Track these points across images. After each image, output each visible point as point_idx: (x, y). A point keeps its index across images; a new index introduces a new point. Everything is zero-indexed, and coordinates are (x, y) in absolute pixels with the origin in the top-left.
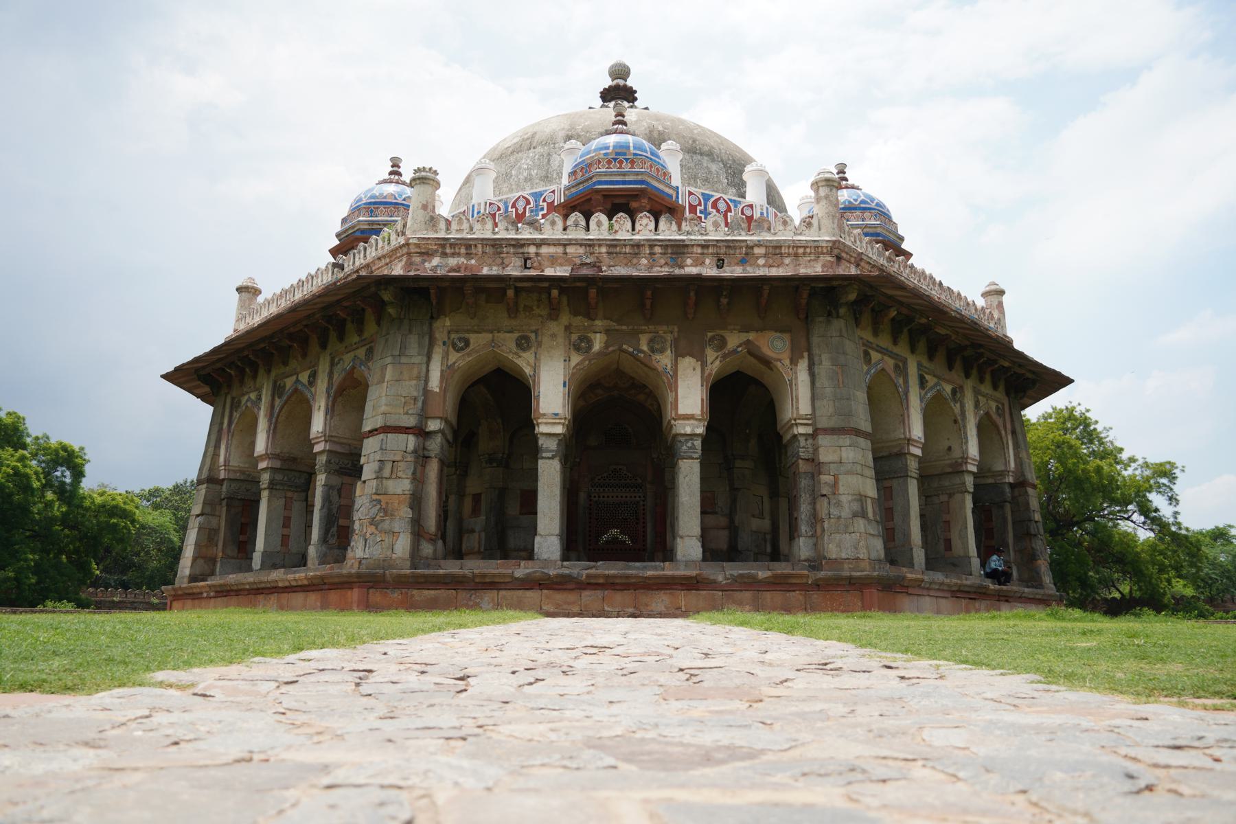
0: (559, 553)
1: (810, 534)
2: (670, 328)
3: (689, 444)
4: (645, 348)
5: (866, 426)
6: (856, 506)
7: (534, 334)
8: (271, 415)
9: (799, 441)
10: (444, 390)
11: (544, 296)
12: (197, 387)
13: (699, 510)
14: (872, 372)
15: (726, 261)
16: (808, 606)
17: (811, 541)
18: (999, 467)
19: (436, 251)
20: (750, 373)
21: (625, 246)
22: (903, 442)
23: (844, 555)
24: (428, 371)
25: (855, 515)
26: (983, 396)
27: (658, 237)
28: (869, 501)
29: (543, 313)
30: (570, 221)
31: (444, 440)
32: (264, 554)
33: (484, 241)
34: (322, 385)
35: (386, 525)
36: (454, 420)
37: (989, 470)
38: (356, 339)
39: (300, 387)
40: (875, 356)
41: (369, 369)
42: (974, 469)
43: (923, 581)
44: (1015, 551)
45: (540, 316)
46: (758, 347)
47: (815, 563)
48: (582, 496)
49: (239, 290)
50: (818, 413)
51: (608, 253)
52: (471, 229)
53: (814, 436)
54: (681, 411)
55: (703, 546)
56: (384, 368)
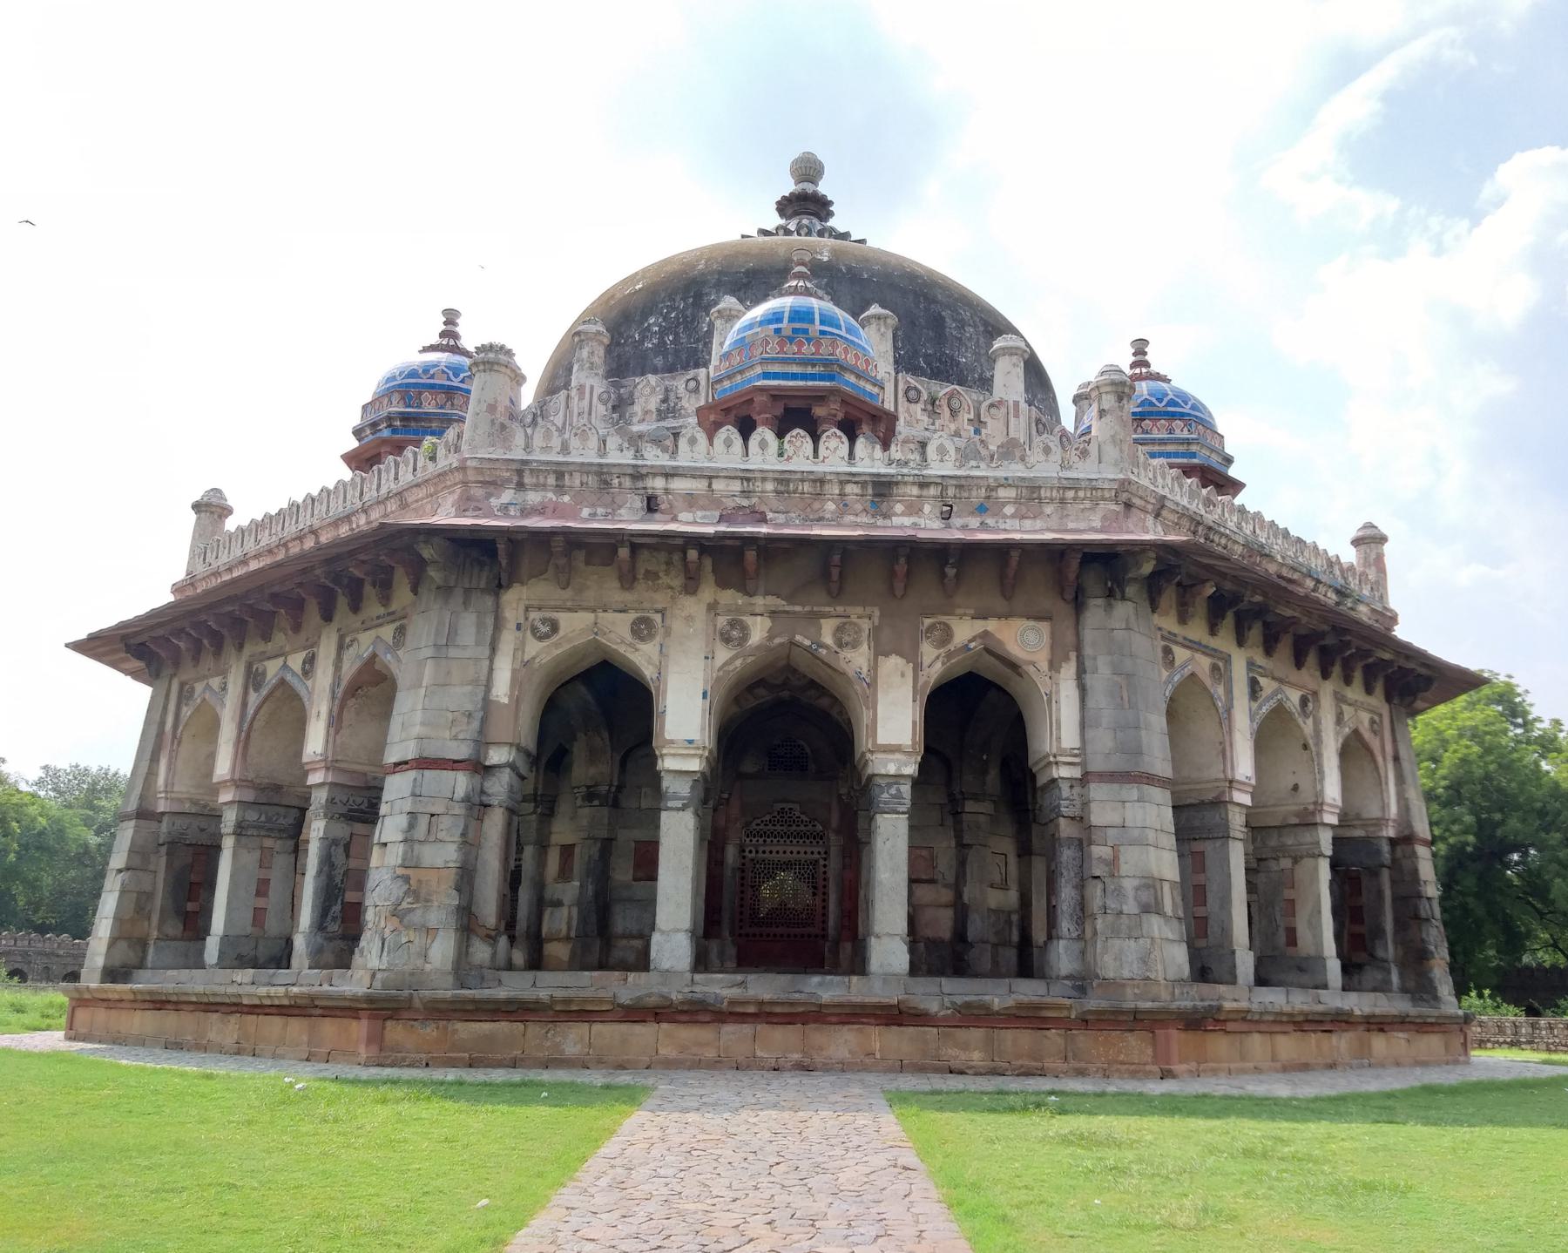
0: (688, 960)
1: (1074, 935)
2: (869, 610)
3: (893, 791)
4: (828, 639)
5: (1163, 768)
7: (660, 615)
9: (1060, 789)
10: (517, 701)
11: (676, 557)
12: (123, 660)
13: (905, 876)
14: (1176, 679)
15: (955, 509)
16: (1070, 1055)
17: (1078, 946)
18: (1373, 811)
19: (509, 481)
20: (989, 676)
21: (803, 481)
22: (1222, 784)
23: (1126, 974)
24: (491, 670)
25: (1145, 909)
26: (1350, 705)
27: (854, 470)
28: (1166, 887)
29: (673, 584)
31: (514, 776)
33: (584, 468)
34: (323, 677)
36: (531, 745)
37: (1358, 817)
38: (382, 611)
39: (289, 677)
40: (1181, 654)
41: (399, 661)
42: (1334, 820)
43: (1249, 1011)
44: (1395, 943)
45: (672, 588)
46: (1000, 642)
47: (1082, 983)
49: (197, 507)
50: (1089, 749)
51: (777, 492)
52: (565, 449)
53: (1085, 780)
54: (881, 741)
55: (912, 951)
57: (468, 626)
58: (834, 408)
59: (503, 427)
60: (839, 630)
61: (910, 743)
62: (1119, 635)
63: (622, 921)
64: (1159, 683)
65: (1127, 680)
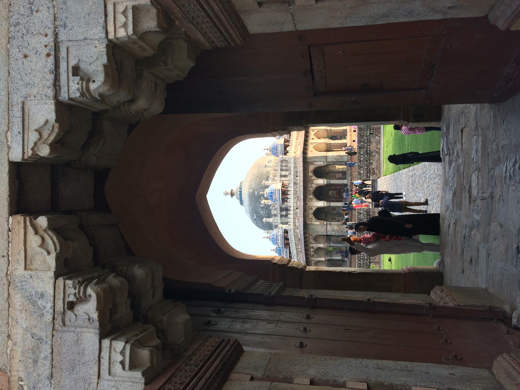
4: (312, 189)
8: (318, 257)
10: (319, 222)
14: (314, 150)
30: (289, 202)
33: (294, 216)
35: (342, 229)
38: (308, 238)
48: (333, 199)
53: (327, 162)
57: (311, 227)
58: (283, 188)
59: (289, 225)
60: (311, 188)
61: (323, 180)
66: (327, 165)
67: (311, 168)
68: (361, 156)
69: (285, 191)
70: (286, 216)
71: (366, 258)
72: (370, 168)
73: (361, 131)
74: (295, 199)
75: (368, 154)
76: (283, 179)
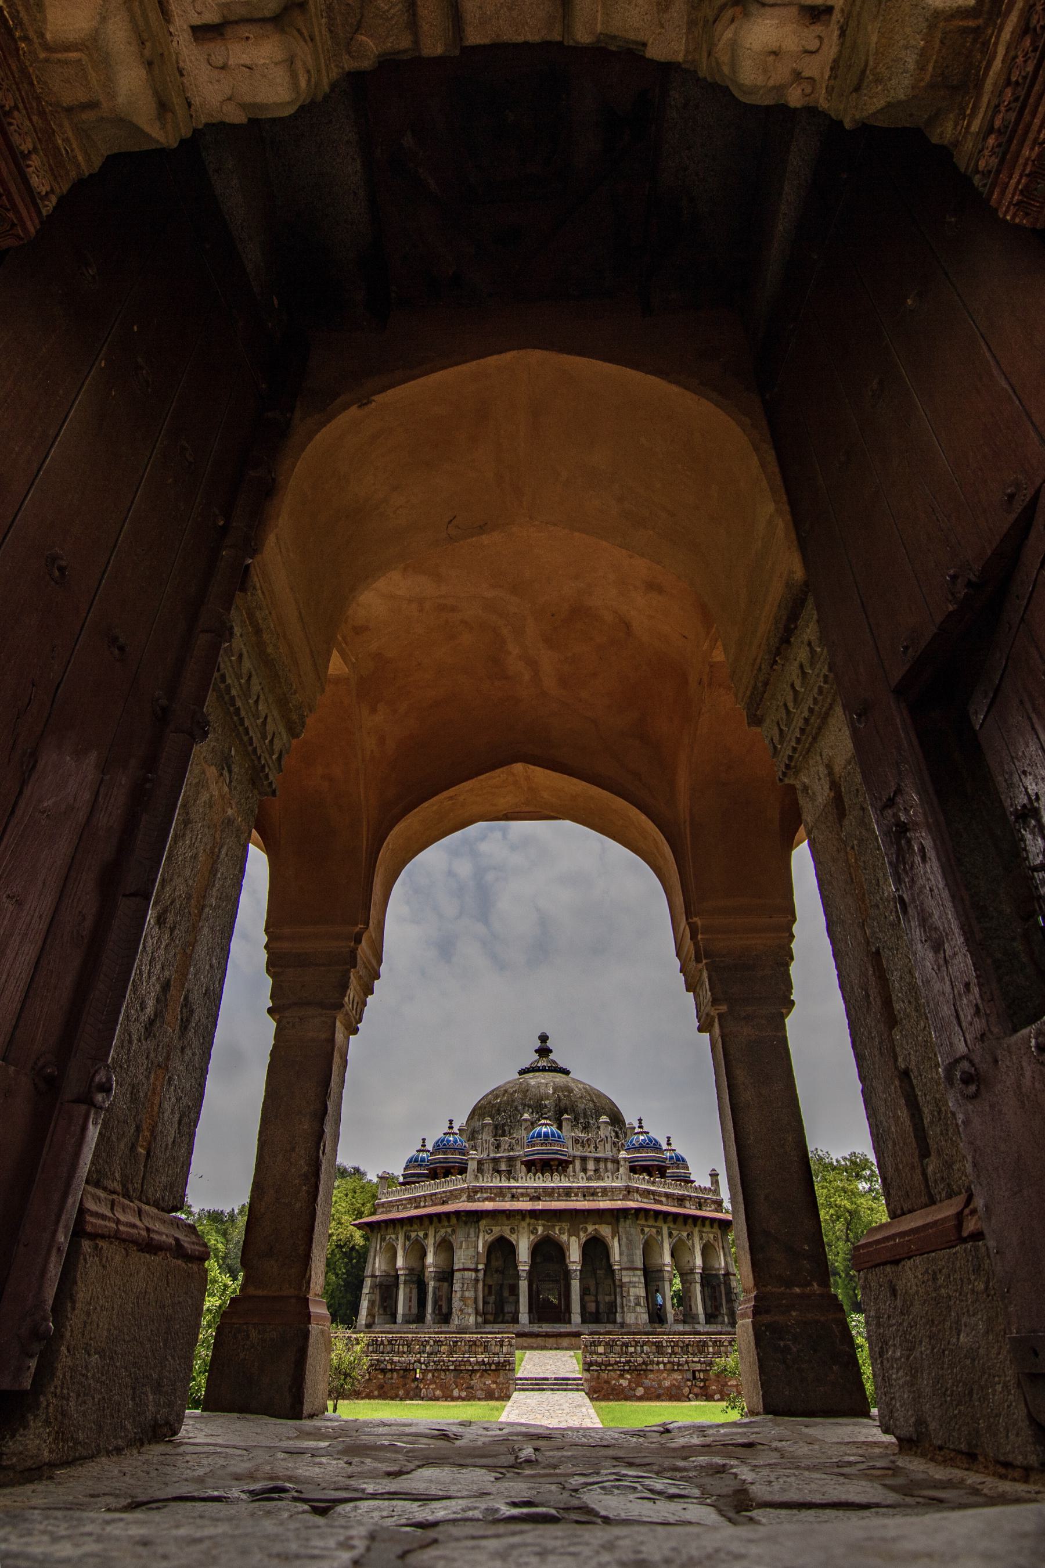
6: (636, 1301)
18: (717, 1266)
32: (403, 1315)
35: (466, 1311)
38: (447, 1224)
40: (646, 1230)
42: (700, 1271)
48: (534, 1286)
53: (621, 1269)
56: (462, 1242)
57: (472, 1231)
58: (556, 1163)
60: (560, 1230)
62: (628, 1229)
63: (508, 1308)
64: (639, 1241)
65: (630, 1242)
66: (613, 1271)
67: (605, 1231)
68: (639, 1348)
69: (551, 1166)
70: (499, 1172)
71: (396, 1359)
72: (609, 1370)
73: (698, 1346)
74: (533, 1191)
75: (644, 1367)
76: (578, 1163)
